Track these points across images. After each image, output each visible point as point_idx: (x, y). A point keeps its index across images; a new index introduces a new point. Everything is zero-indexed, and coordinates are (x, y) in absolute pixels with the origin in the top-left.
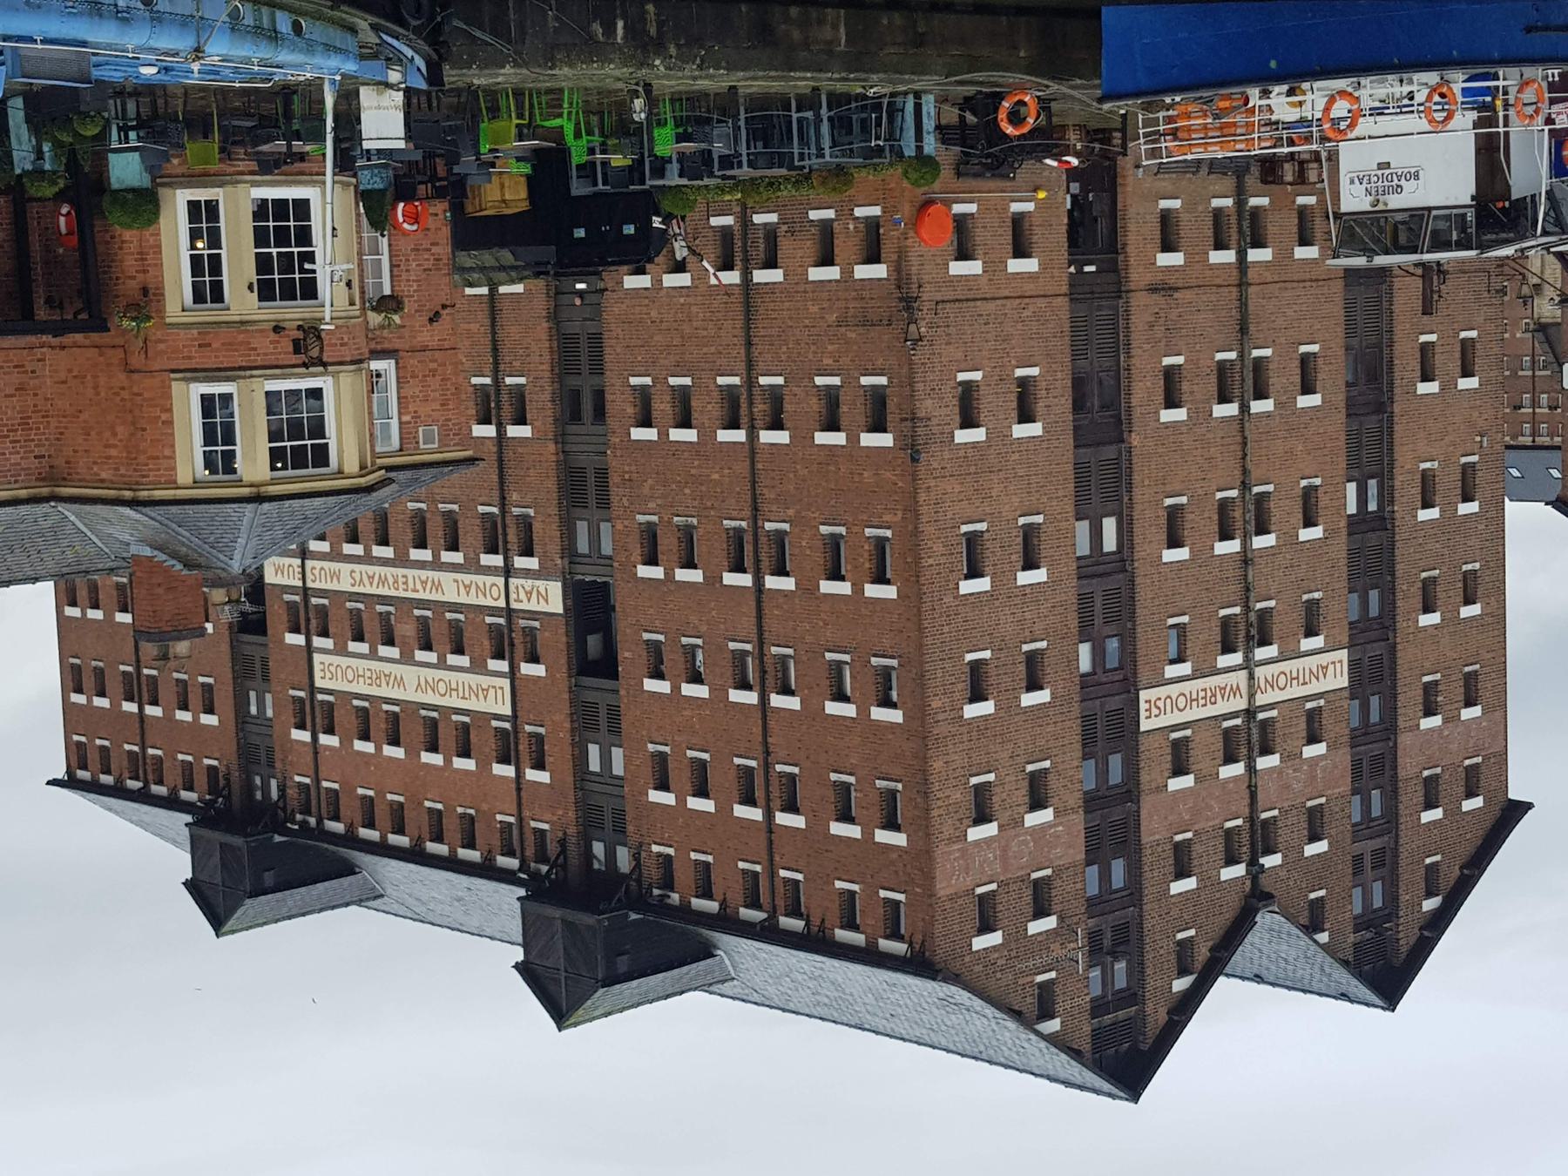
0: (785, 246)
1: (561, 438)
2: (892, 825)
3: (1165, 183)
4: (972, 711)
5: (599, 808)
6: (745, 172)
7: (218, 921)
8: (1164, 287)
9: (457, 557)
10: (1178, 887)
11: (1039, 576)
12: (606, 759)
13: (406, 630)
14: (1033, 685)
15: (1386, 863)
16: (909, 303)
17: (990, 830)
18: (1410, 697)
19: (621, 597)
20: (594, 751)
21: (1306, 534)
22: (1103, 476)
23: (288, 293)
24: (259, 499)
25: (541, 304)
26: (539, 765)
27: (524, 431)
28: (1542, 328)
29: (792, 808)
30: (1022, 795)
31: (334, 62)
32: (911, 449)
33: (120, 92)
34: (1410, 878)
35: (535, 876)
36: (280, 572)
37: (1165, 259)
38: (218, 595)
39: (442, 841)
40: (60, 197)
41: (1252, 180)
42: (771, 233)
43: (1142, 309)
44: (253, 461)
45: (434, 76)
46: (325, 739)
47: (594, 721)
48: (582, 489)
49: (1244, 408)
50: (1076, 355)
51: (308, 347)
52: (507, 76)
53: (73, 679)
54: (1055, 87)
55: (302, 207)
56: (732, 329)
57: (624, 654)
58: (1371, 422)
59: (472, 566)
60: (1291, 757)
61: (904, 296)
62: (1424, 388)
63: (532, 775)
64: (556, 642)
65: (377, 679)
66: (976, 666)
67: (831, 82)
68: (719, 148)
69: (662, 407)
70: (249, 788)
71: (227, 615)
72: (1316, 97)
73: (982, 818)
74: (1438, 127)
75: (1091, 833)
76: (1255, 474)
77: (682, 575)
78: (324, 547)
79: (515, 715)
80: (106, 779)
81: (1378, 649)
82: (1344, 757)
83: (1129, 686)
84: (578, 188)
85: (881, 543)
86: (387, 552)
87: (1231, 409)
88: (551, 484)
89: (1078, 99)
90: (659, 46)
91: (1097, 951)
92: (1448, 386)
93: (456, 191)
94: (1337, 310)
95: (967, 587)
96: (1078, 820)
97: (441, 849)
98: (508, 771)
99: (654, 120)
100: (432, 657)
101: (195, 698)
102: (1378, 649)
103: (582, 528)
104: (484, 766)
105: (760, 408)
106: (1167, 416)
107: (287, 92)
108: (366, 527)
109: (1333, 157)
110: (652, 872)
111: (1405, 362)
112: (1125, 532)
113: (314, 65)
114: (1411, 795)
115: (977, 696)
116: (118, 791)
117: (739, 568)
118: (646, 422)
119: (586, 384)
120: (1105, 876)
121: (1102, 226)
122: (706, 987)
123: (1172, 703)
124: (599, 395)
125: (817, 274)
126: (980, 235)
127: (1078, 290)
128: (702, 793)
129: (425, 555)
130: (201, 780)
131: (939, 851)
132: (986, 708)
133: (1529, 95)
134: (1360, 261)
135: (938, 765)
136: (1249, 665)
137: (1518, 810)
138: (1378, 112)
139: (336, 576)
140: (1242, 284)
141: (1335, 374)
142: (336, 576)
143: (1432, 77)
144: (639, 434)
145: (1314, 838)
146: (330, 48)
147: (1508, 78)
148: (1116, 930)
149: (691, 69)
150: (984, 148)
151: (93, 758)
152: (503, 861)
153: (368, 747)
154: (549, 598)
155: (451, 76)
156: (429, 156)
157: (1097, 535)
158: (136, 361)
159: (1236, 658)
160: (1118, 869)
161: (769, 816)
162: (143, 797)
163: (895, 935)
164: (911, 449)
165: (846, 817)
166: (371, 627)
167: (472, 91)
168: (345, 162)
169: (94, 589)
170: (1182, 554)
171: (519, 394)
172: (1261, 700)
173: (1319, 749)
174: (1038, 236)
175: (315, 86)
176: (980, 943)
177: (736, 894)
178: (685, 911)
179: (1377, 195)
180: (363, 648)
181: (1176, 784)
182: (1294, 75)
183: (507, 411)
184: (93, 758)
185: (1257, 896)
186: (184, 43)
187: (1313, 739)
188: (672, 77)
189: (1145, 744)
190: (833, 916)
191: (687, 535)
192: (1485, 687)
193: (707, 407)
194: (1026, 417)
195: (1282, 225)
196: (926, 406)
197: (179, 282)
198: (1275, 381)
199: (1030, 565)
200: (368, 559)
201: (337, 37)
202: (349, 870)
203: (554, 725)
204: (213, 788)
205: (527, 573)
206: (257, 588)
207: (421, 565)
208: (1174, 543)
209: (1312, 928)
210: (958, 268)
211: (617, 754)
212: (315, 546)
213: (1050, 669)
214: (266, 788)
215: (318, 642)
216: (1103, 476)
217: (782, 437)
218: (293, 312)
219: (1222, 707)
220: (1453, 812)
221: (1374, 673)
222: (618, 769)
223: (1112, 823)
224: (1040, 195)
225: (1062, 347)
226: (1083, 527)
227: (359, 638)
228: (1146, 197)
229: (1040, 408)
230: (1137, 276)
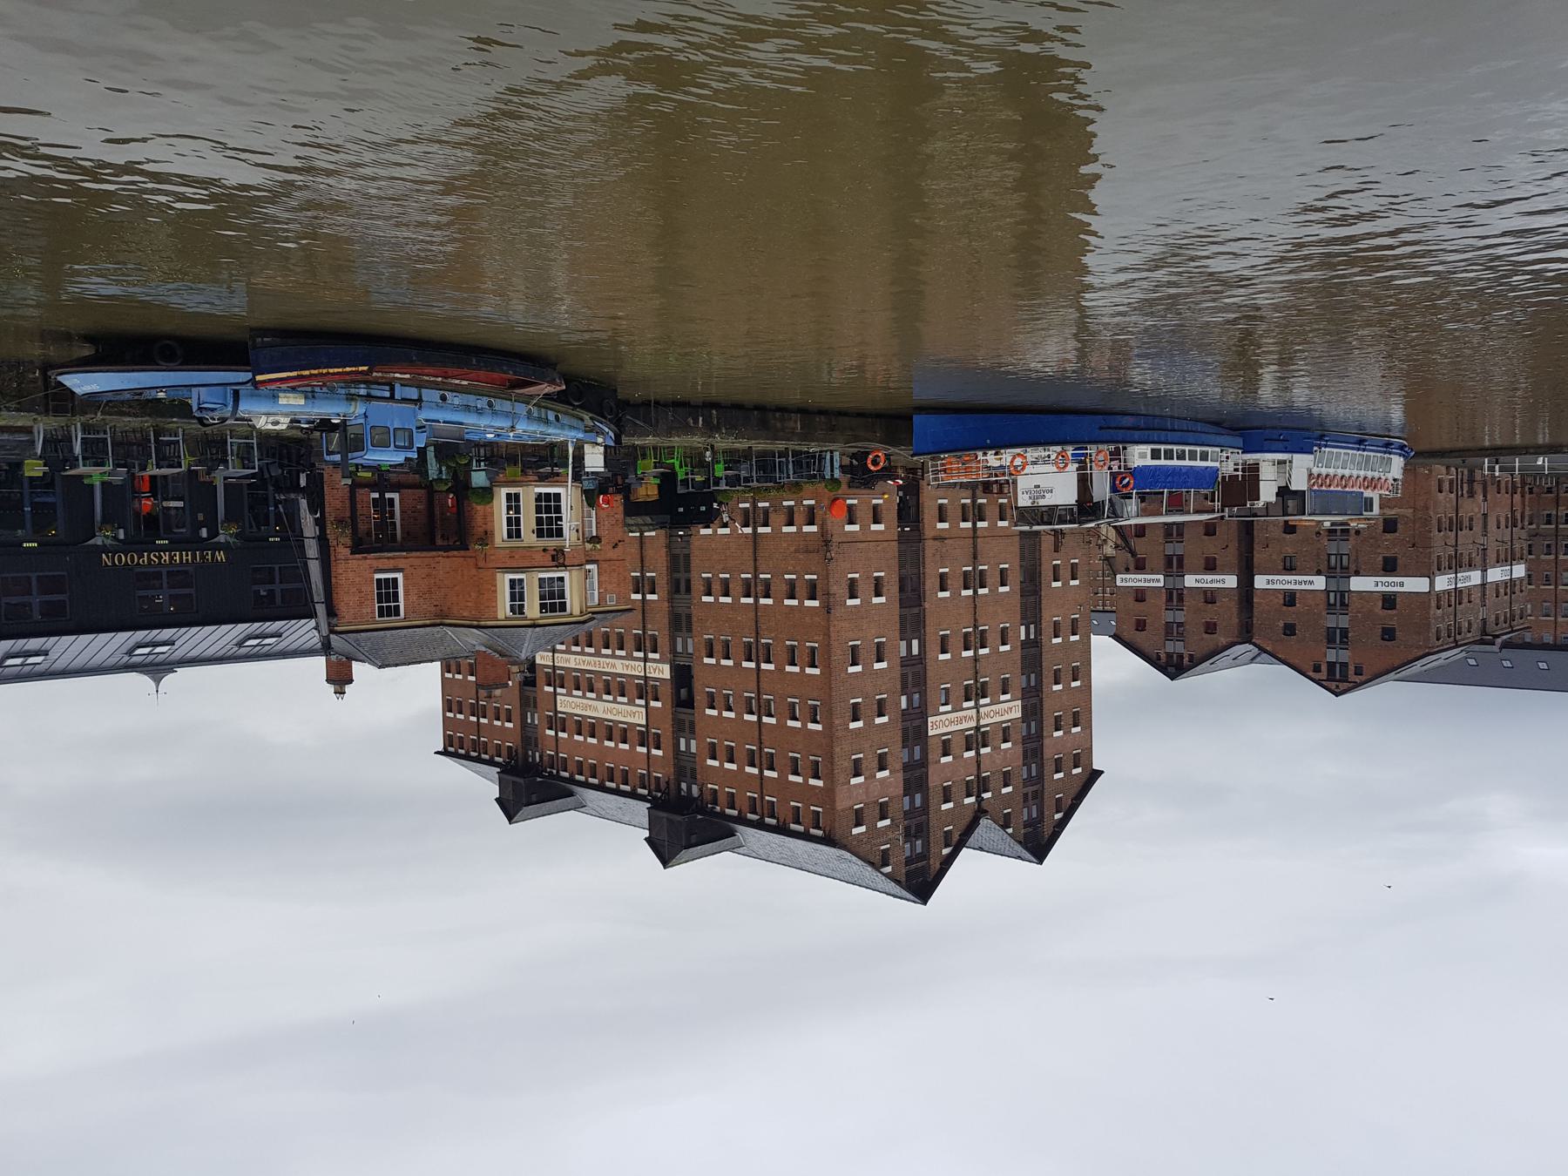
0: (772, 517)
1: (671, 600)
2: (817, 777)
3: (940, 492)
4: (853, 725)
5: (684, 767)
6: (755, 484)
7: (511, 818)
8: (940, 538)
9: (623, 653)
10: (945, 807)
11: (884, 665)
12: (688, 745)
13: (599, 685)
14: (881, 715)
15: (1038, 796)
16: (827, 543)
17: (861, 779)
18: (1048, 722)
19: (696, 671)
20: (683, 741)
21: (1003, 648)
22: (912, 618)
23: (550, 535)
24: (534, 626)
25: (663, 541)
26: (658, 748)
27: (654, 597)
28: (1107, 559)
29: (771, 768)
30: (875, 764)
31: (573, 433)
32: (827, 608)
33: (478, 445)
34: (1049, 804)
35: (654, 798)
36: (543, 658)
37: (940, 526)
38: (515, 669)
39: (613, 781)
40: (449, 491)
41: (979, 492)
42: (766, 511)
43: (930, 547)
44: (532, 609)
45: (618, 440)
46: (561, 734)
47: (683, 728)
48: (680, 623)
49: (975, 592)
50: (901, 566)
51: (558, 558)
52: (650, 440)
53: (448, 706)
54: (893, 450)
55: (557, 496)
56: (749, 553)
57: (697, 698)
58: (1032, 599)
59: (629, 657)
60: (996, 748)
61: (825, 540)
62: (1055, 584)
63: (654, 752)
64: (666, 691)
65: (586, 707)
66: (855, 705)
67: (793, 446)
68: (743, 474)
69: (716, 587)
70: (526, 756)
71: (519, 678)
72: (1007, 456)
73: (857, 775)
74: (1061, 470)
75: (907, 782)
76: (980, 621)
77: (724, 662)
78: (563, 647)
79: (647, 726)
80: (462, 751)
81: (1034, 700)
82: (1020, 749)
83: (924, 717)
84: (681, 490)
85: (813, 649)
86: (592, 650)
87: (970, 592)
88: (666, 621)
89: (902, 455)
90: (717, 429)
91: (909, 836)
92: (1065, 584)
93: (626, 491)
94: (1016, 549)
95: (852, 669)
96: (900, 775)
97: (613, 785)
98: (644, 750)
99: (715, 461)
100: (610, 698)
101: (503, 716)
102: (1034, 700)
103: (679, 640)
104: (633, 747)
105: (760, 588)
106: (941, 595)
107: (552, 445)
108: (582, 639)
109: (1015, 482)
110: (708, 797)
111: (1047, 572)
112: (922, 646)
113: (564, 434)
114: (1049, 766)
115: (855, 719)
116: (467, 757)
117: (750, 660)
118: (709, 594)
119: (682, 576)
120: (912, 801)
121: (913, 510)
122: (732, 850)
123: (942, 723)
124: (688, 582)
125: (786, 529)
126: (859, 514)
127: (902, 539)
128: (731, 761)
129: (609, 652)
130: (504, 752)
131: (838, 789)
132: (859, 724)
133: (1101, 457)
134: (1027, 528)
135: (837, 750)
136: (977, 707)
137: (1097, 774)
138: (1034, 463)
139: (568, 661)
140: (975, 537)
141: (1015, 577)
142: (568, 661)
143: (1058, 449)
144: (705, 599)
145: (1006, 785)
146: (572, 427)
147: (1092, 449)
148: (917, 825)
149: (731, 439)
150: (860, 476)
151: (456, 742)
152: (640, 791)
153: (581, 738)
154: (664, 672)
155: (625, 440)
156: (615, 475)
157: (909, 647)
158: (481, 564)
159: (972, 704)
160: (918, 797)
161: (761, 772)
162: (478, 760)
163: (818, 827)
164: (827, 608)
165: (796, 773)
166: (583, 684)
167: (634, 447)
168: (577, 477)
169: (458, 665)
170: (947, 656)
171: (652, 580)
172: (982, 722)
173: (1009, 745)
174: (884, 514)
175: (564, 444)
176: (856, 831)
177: (745, 808)
178: (723, 815)
179: (1034, 499)
180: (580, 693)
181: (944, 760)
182: (998, 447)
183: (647, 588)
184: (456, 742)
185: (980, 812)
186: (506, 424)
187: (1005, 741)
188: (722, 442)
189: (930, 741)
190: (790, 816)
191: (727, 644)
192: (1082, 718)
193: (736, 588)
194: (878, 594)
195: (992, 512)
196: (834, 589)
197: (501, 529)
198: (989, 580)
199: (879, 660)
200: (582, 653)
201: (575, 422)
202: (571, 794)
203: (664, 729)
204: (510, 756)
205: (654, 661)
206: (532, 666)
207: (607, 656)
208: (944, 651)
209: (1005, 826)
210: (848, 528)
211: (693, 742)
212: (559, 647)
213: (888, 706)
214: (534, 757)
215: (559, 690)
216: (912, 618)
217: (769, 601)
218: (552, 543)
219: (965, 725)
220: (1068, 774)
221: (1033, 711)
222: (693, 750)
223: (915, 777)
224: (885, 497)
225: (895, 563)
226: (903, 644)
227: (578, 689)
228: (932, 498)
229: (885, 590)
230: (928, 533)
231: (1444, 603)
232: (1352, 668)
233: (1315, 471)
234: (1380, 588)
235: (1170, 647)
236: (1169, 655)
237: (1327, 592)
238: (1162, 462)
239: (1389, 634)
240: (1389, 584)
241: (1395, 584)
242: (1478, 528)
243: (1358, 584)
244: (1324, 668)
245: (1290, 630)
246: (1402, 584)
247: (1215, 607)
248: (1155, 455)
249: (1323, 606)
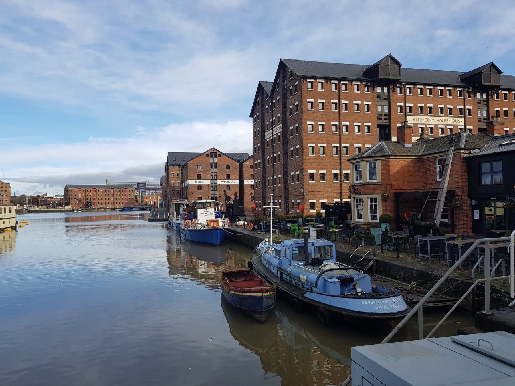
123: (278, 129)
232: (209, 156)
234: (202, 181)
237: (217, 179)
240: (199, 182)
241: (198, 182)
243: (208, 182)
245: (228, 167)
249: (218, 175)
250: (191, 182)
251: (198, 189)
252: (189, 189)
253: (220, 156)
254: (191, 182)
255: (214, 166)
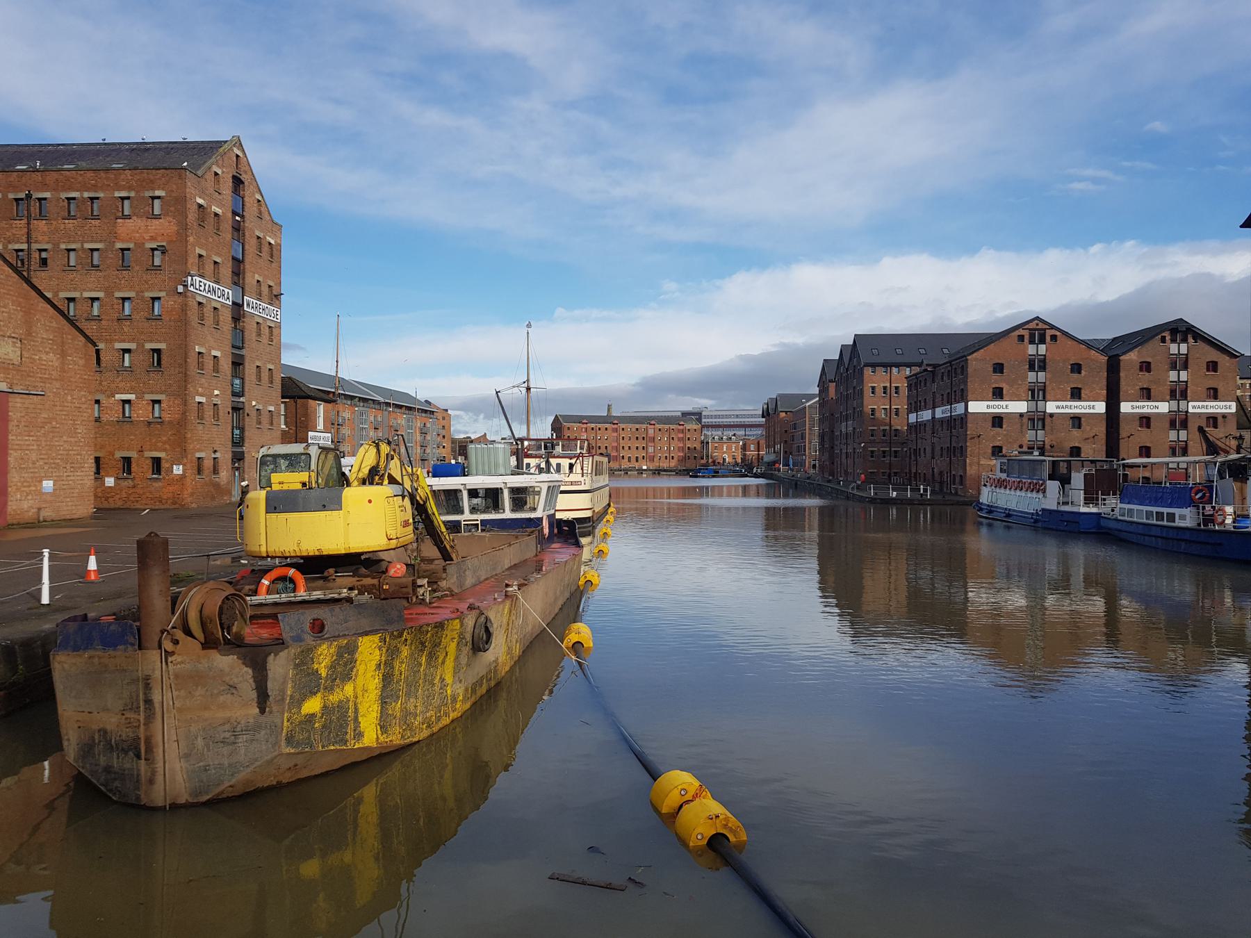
231: (958, 393)
232: (1027, 340)
233: (1041, 495)
235: (1184, 348)
236: (1185, 340)
237: (1044, 399)
238: (1165, 510)
239: (999, 368)
240: (998, 407)
242: (938, 449)
243: (1020, 407)
244: (1048, 338)
245: (1077, 368)
246: (988, 407)
247: (1141, 385)
248: (1171, 517)
249: (1048, 389)
250: (976, 407)
251: (993, 426)
252: (969, 425)
253: (1054, 338)
254: (976, 407)
255: (1038, 364)
